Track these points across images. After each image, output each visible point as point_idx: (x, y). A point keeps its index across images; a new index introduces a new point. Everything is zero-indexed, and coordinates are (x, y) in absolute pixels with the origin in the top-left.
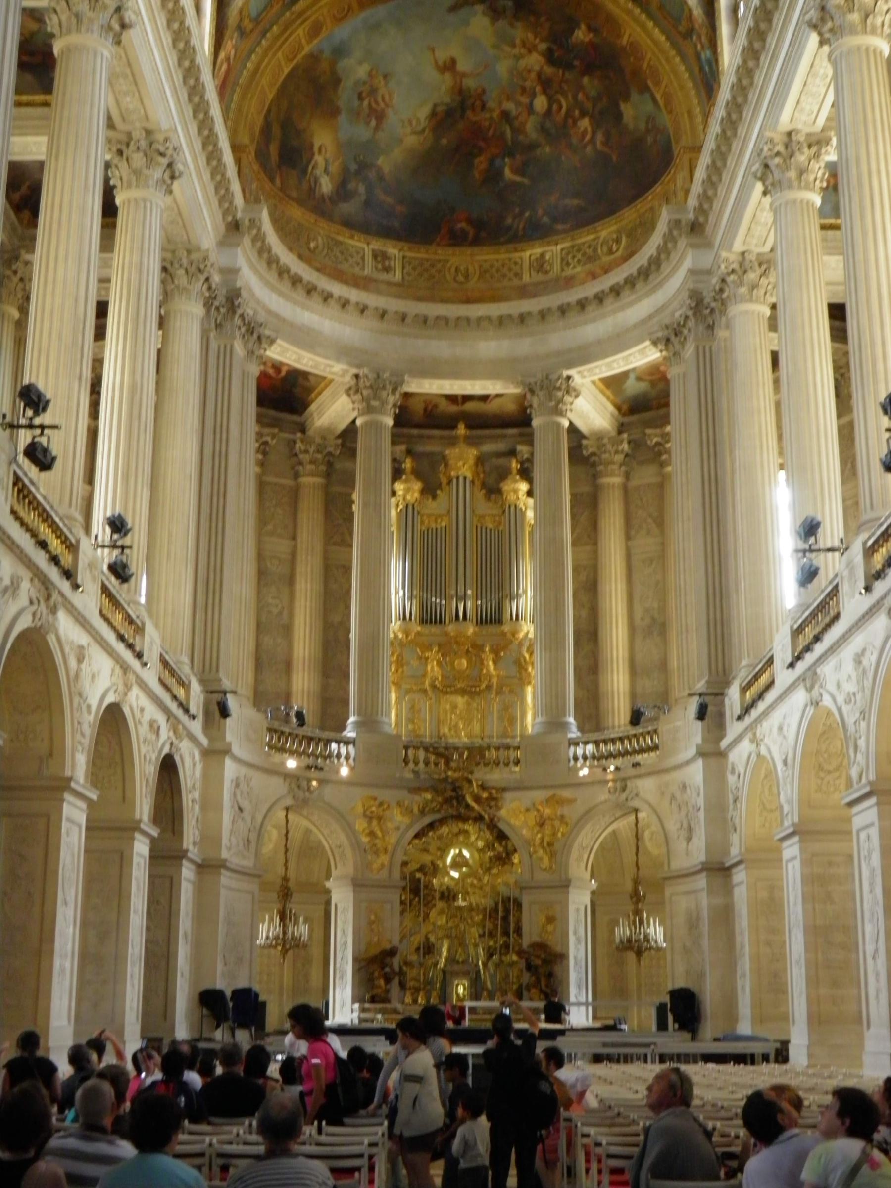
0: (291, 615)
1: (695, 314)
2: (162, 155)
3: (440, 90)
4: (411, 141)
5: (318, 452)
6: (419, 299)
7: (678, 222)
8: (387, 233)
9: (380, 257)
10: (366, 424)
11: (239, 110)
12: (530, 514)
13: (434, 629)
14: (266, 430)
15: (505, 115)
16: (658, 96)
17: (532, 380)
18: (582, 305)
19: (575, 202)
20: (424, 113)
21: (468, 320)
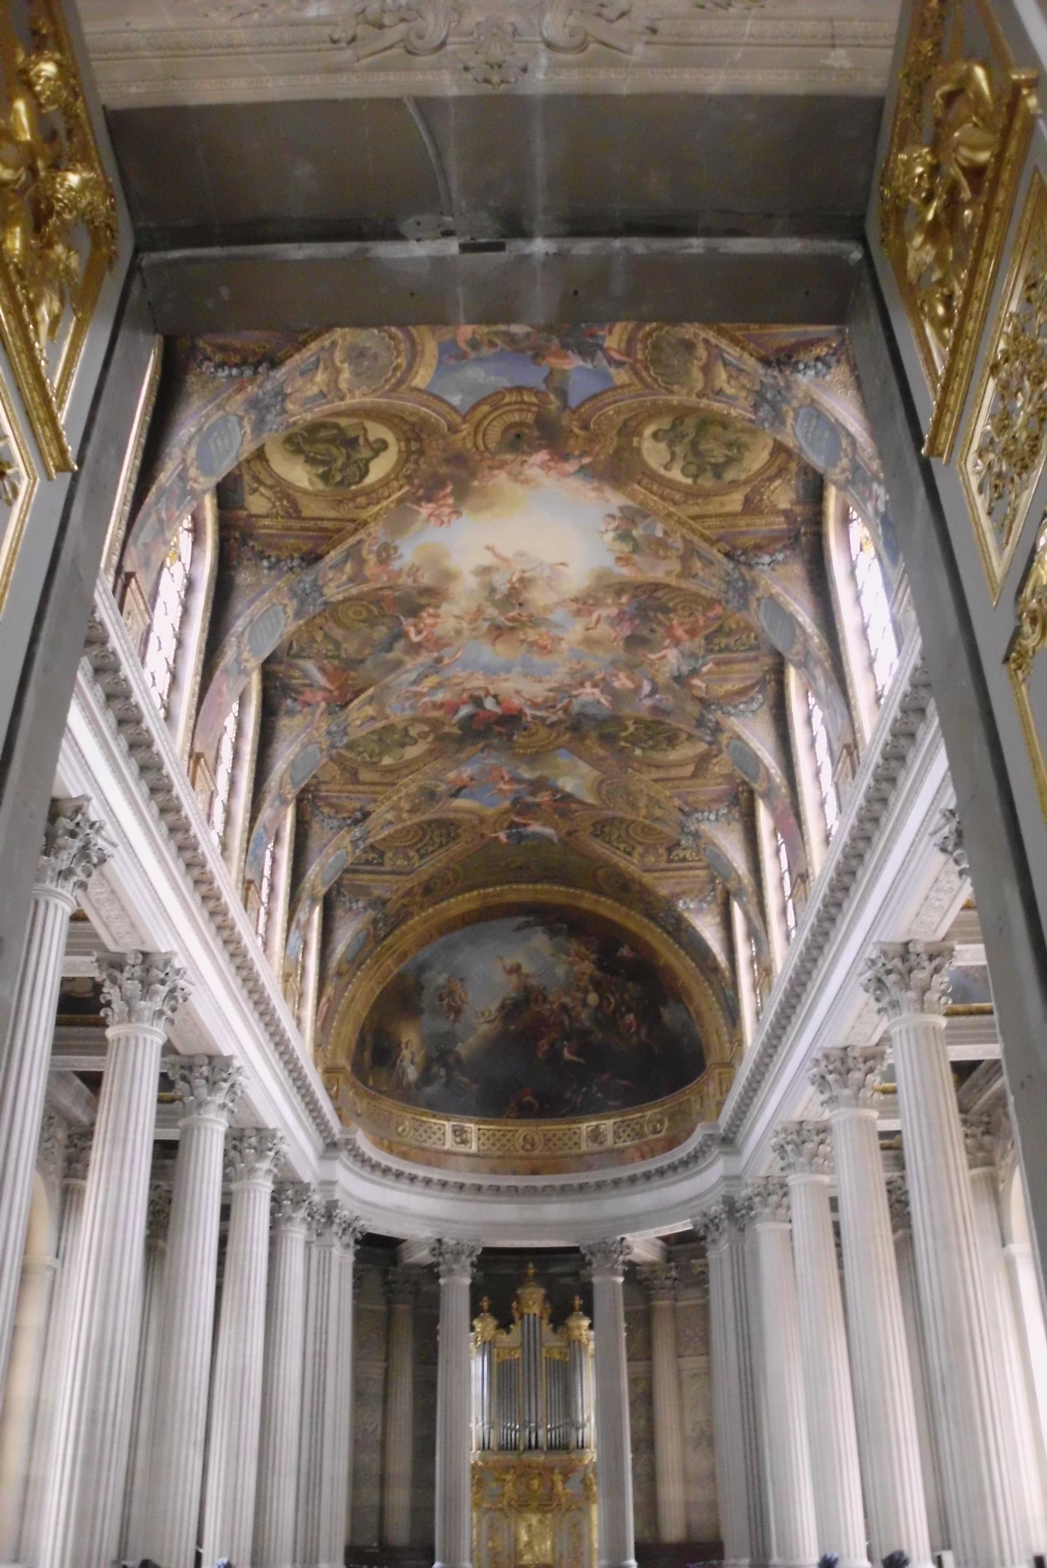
0: (384, 1434)
1: (728, 1218)
2: (270, 1150)
3: (506, 987)
4: (484, 1028)
5: (406, 1282)
6: (493, 1171)
7: (711, 1136)
8: (465, 1111)
9: (458, 1132)
10: (447, 1285)
11: (338, 1035)
12: (591, 1346)
13: (510, 1457)
14: (361, 1266)
15: (564, 1007)
16: (691, 1009)
17: (591, 1242)
18: (633, 1180)
19: (624, 1082)
20: (494, 1006)
21: (534, 1188)
